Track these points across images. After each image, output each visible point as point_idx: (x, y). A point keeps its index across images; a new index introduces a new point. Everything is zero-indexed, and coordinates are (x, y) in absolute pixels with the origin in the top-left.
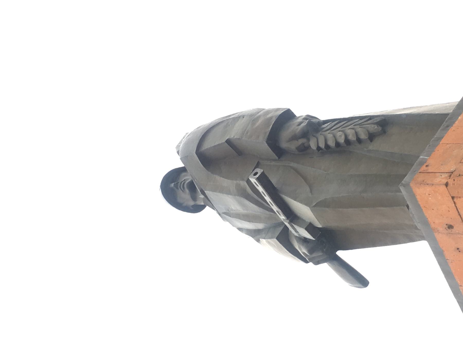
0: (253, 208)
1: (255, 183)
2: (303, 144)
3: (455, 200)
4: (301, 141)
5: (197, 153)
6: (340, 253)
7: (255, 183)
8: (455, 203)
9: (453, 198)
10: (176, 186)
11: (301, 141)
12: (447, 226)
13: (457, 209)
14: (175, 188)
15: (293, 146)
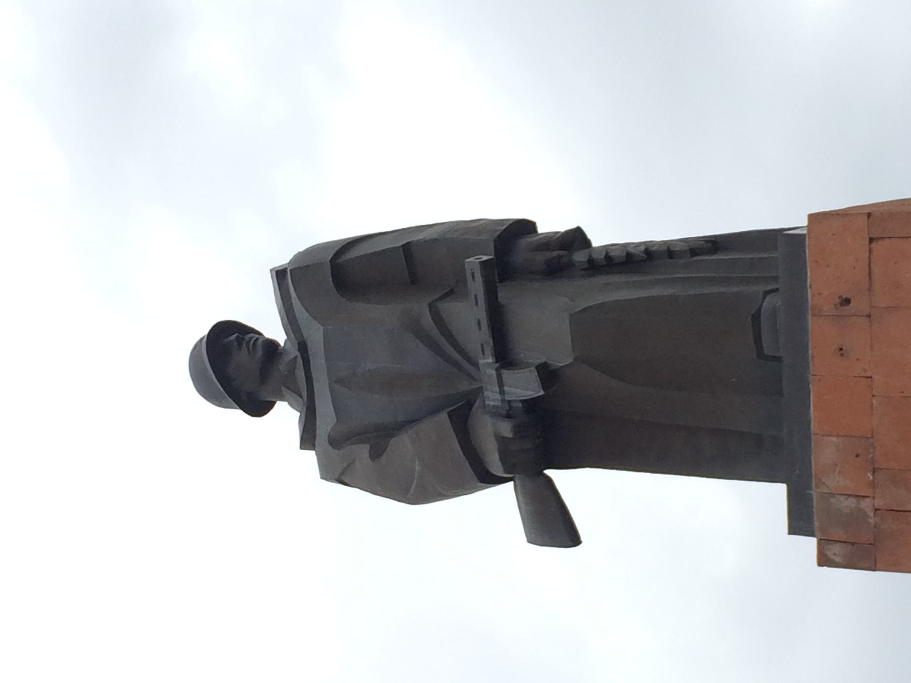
0: (421, 358)
1: (473, 274)
2: (560, 257)
3: (873, 245)
4: (555, 253)
5: (333, 260)
6: (548, 472)
7: (473, 274)
8: (870, 251)
9: (871, 240)
10: (240, 341)
11: (555, 253)
12: (838, 301)
13: (870, 263)
14: (236, 344)
15: (541, 257)
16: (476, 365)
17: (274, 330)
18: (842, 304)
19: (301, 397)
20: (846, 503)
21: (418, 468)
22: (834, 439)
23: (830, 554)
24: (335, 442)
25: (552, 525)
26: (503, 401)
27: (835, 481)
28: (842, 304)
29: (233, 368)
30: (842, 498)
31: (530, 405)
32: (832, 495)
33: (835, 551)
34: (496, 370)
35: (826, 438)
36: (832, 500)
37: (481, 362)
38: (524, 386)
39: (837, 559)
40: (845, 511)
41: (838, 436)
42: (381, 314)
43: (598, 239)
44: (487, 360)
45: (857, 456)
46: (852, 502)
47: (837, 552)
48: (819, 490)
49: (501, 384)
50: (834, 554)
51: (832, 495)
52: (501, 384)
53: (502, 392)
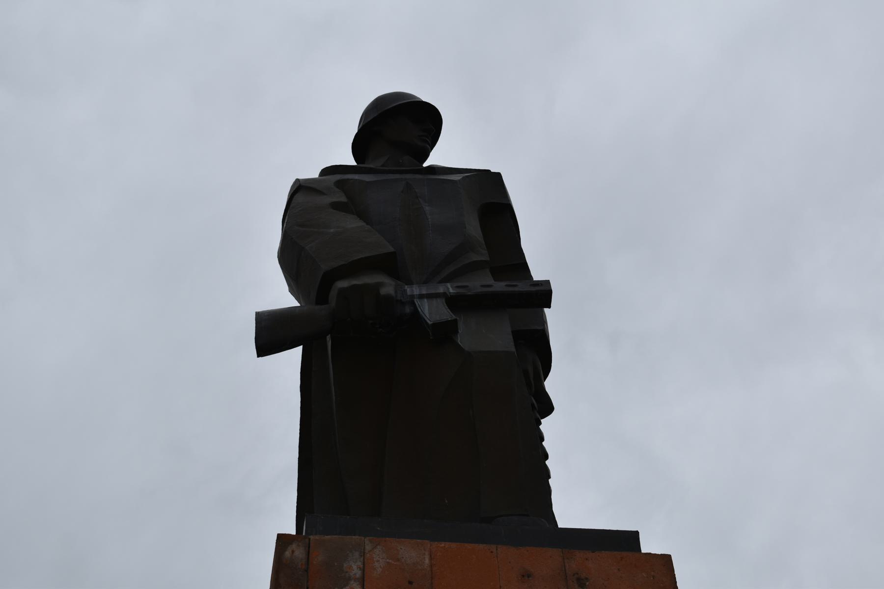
16: (441, 282)
17: (437, 157)
18: (578, 579)
19: (383, 166)
20: (355, 567)
21: (332, 230)
22: (427, 561)
23: (294, 546)
24: (339, 184)
25: (271, 334)
26: (413, 296)
27: (379, 558)
28: (578, 579)
29: (399, 127)
30: (360, 564)
31: (416, 315)
32: (363, 554)
33: (297, 552)
34: (445, 293)
35: (427, 553)
36: (357, 554)
37: (449, 285)
38: (433, 312)
39: (288, 554)
40: (345, 565)
41: (431, 566)
42: (473, 228)
43: (547, 425)
44: (451, 289)
45: (410, 583)
46: (356, 571)
47: (297, 553)
48: (367, 541)
49: (430, 296)
50: (293, 552)
51: (363, 554)
52: (430, 296)
53: (421, 297)
